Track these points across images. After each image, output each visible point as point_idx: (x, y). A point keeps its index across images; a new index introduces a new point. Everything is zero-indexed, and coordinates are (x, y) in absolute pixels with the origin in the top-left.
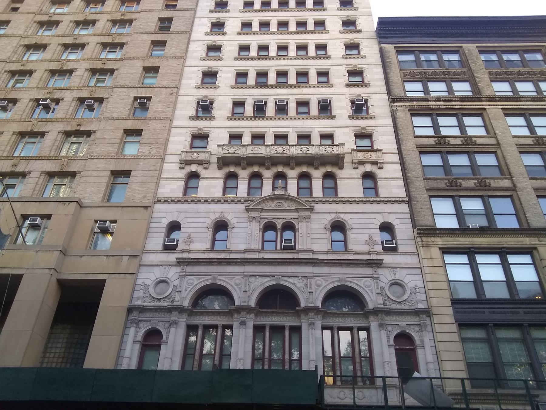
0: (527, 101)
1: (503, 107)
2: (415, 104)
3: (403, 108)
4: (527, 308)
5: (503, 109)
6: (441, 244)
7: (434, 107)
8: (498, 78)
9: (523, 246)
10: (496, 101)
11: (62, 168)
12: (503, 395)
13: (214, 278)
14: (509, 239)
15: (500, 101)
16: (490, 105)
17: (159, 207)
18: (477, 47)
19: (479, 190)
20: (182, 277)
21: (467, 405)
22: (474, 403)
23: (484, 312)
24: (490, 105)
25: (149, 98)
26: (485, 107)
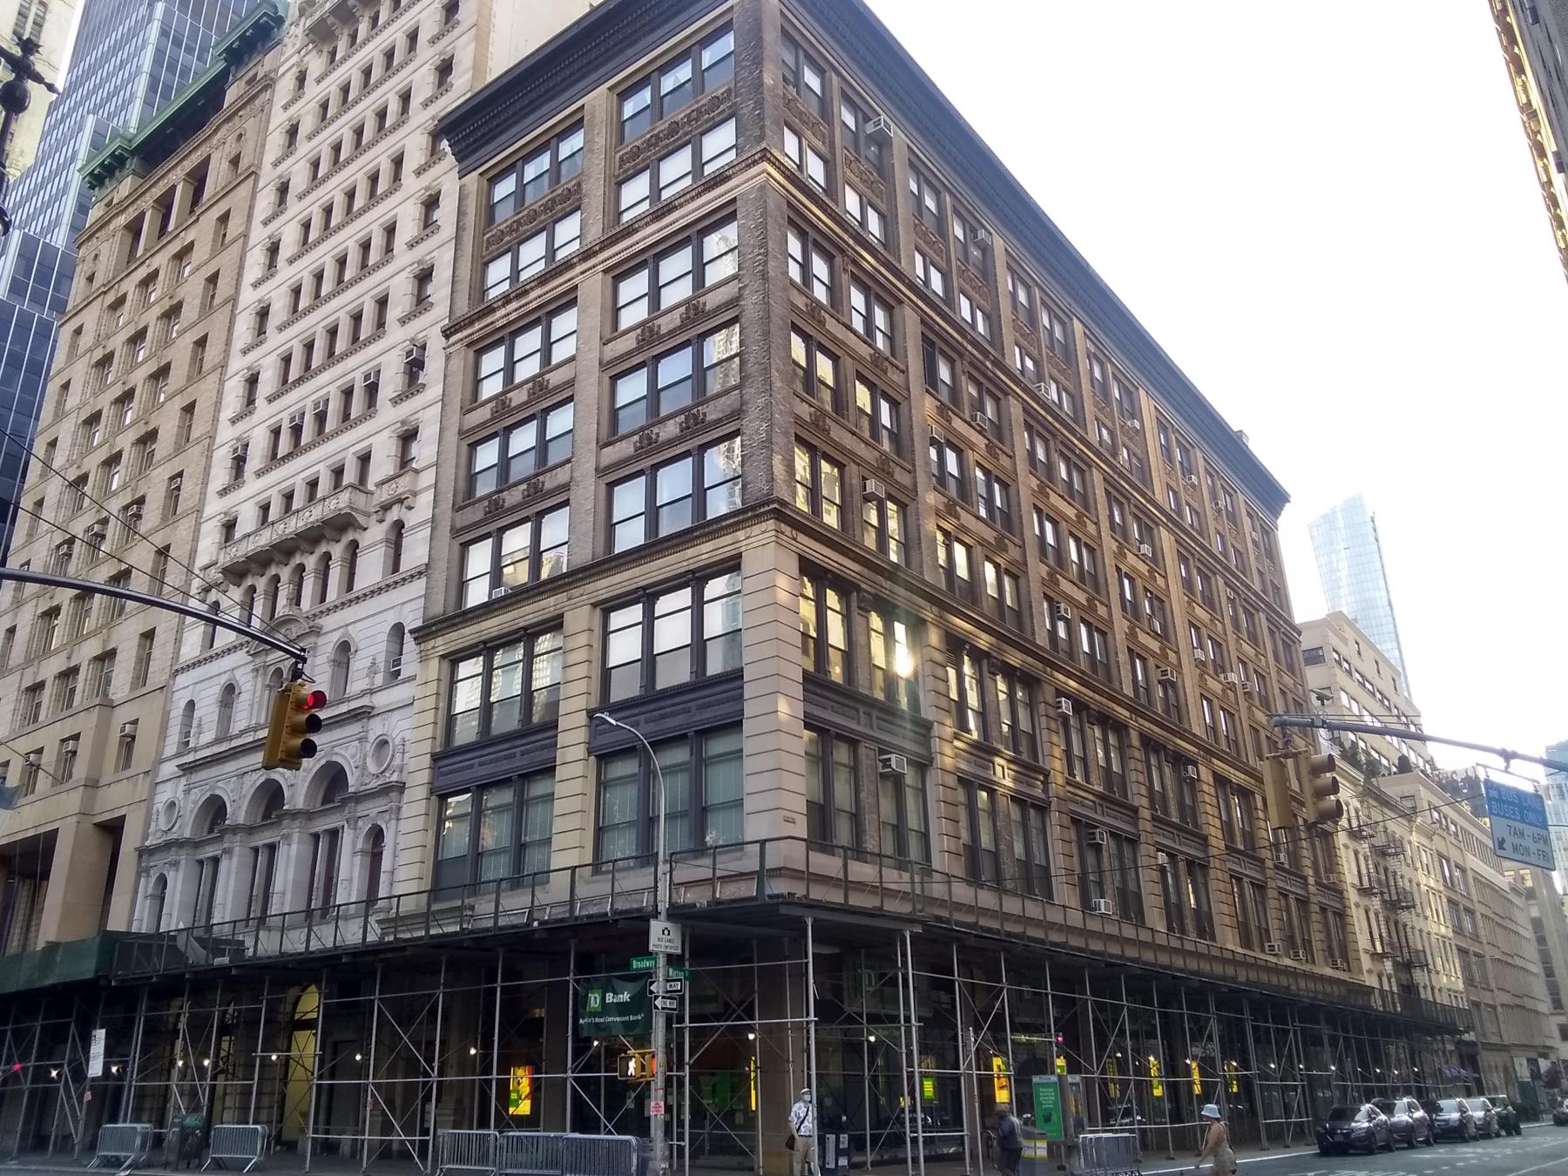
0: (647, 224)
1: (601, 268)
2: (477, 326)
3: (459, 346)
4: (482, 756)
5: (605, 271)
6: (442, 650)
7: (499, 324)
8: (638, 164)
9: (545, 617)
10: (595, 254)
11: (104, 647)
12: (440, 912)
13: (213, 788)
14: (529, 609)
15: (602, 250)
16: (583, 273)
17: (182, 680)
18: (609, 89)
19: (693, 435)
20: (187, 792)
21: (427, 931)
22: (403, 931)
23: (471, 767)
24: (583, 273)
25: (180, 475)
26: (576, 281)
